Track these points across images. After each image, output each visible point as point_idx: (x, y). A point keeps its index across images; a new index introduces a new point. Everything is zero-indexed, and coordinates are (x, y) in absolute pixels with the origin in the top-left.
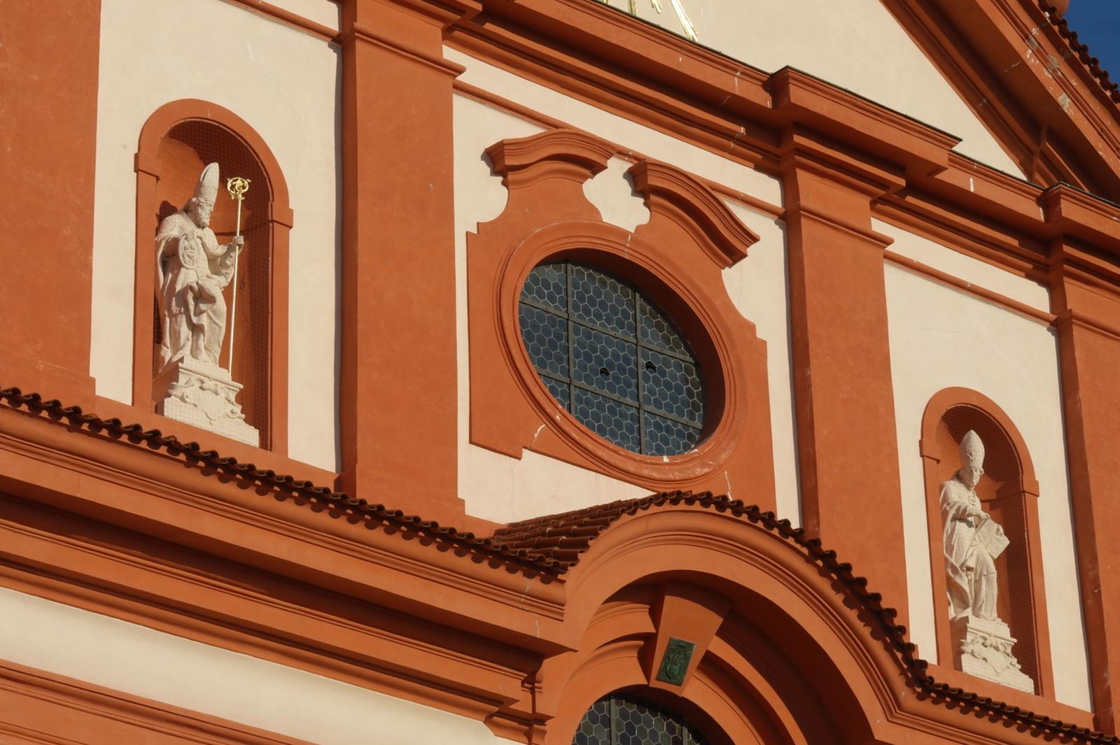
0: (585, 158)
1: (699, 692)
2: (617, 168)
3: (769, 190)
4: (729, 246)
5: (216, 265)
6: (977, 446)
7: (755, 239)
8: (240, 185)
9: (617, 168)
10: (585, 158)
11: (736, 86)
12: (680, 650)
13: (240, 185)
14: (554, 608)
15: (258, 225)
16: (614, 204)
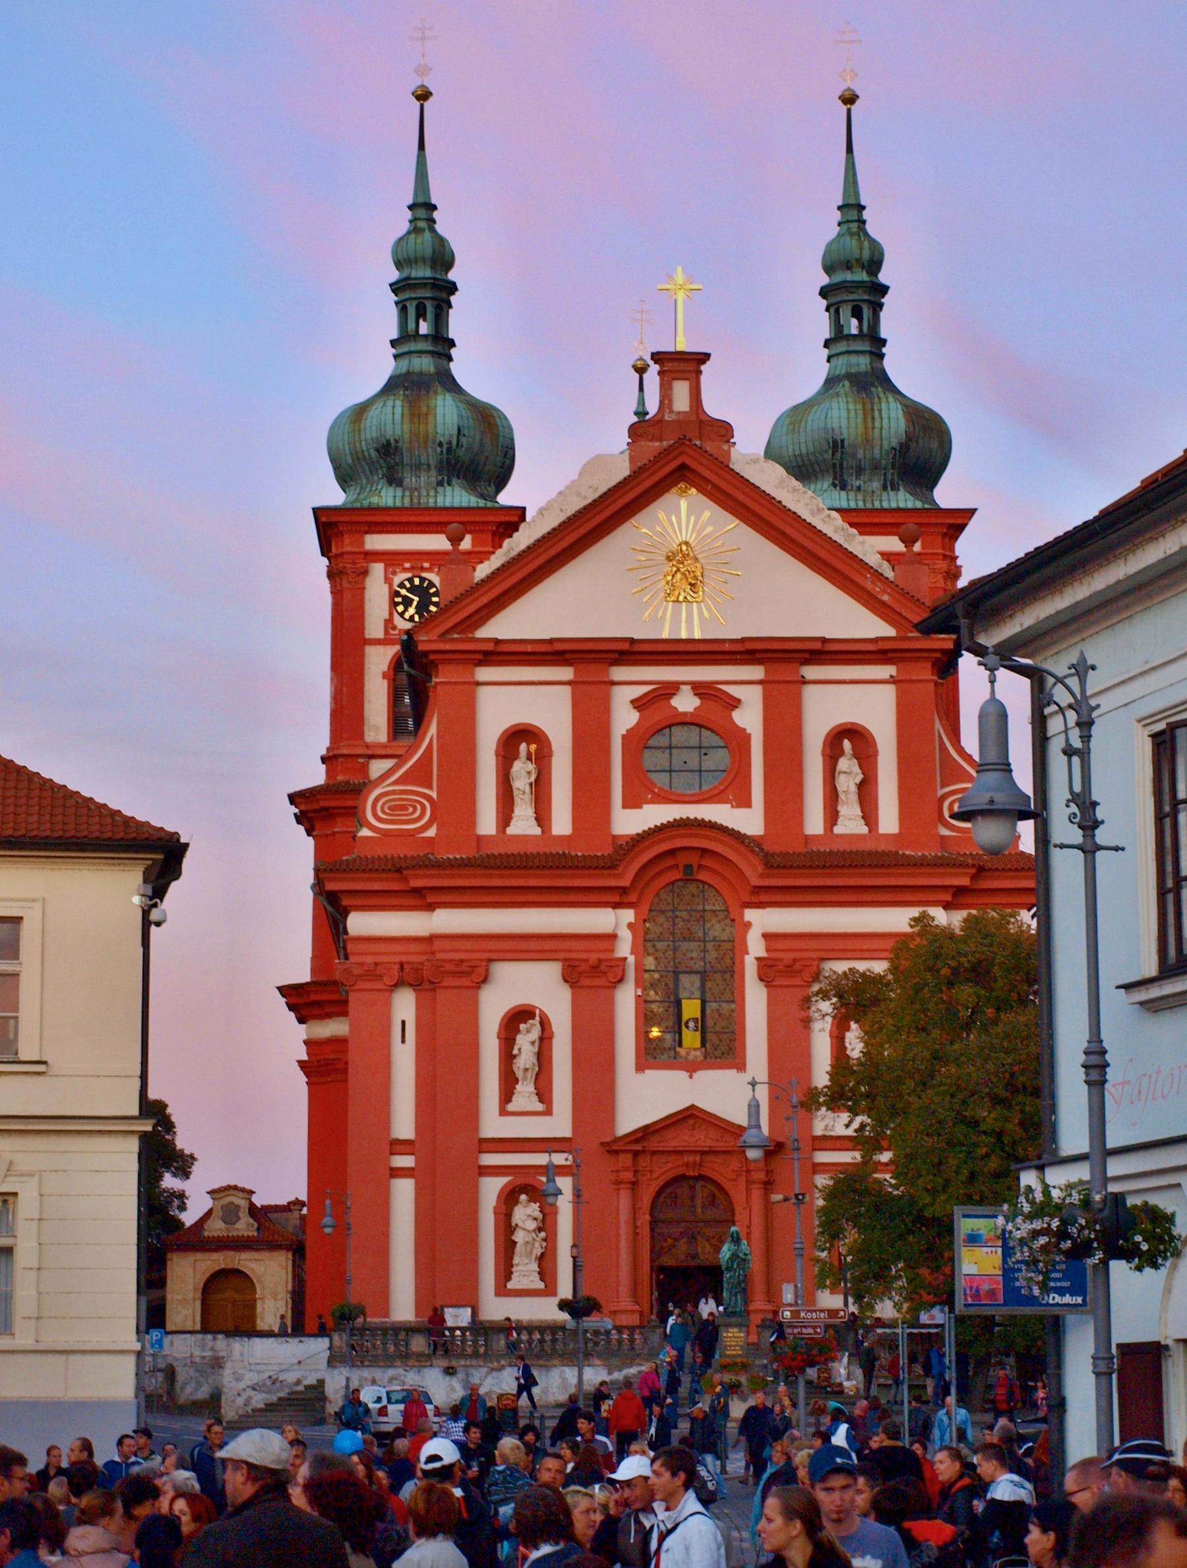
0: (671, 689)
1: (702, 876)
2: (686, 689)
3: (756, 672)
4: (735, 703)
5: (529, 773)
6: (847, 744)
7: (739, 701)
8: (533, 747)
9: (686, 689)
10: (671, 689)
11: (727, 647)
12: (688, 868)
13: (533, 747)
14: (620, 876)
15: (542, 759)
16: (685, 702)
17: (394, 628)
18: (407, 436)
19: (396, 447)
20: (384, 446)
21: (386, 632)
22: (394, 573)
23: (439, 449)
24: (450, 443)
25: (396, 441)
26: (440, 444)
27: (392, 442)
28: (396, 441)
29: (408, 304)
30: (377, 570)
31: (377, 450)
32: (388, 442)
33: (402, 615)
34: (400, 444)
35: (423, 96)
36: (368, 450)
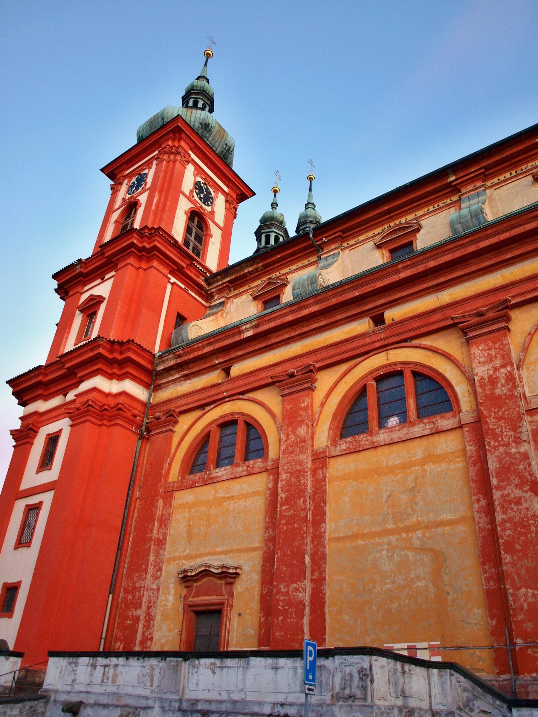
17: (193, 196)
18: (216, 130)
19: (210, 130)
20: (206, 124)
21: (190, 195)
22: (197, 175)
23: (225, 146)
24: (230, 147)
25: (211, 127)
26: (226, 145)
27: (210, 125)
28: (211, 127)
29: (200, 101)
30: (190, 168)
31: (201, 124)
32: (209, 124)
33: (197, 194)
34: (213, 130)
35: (208, 56)
36: (194, 122)
